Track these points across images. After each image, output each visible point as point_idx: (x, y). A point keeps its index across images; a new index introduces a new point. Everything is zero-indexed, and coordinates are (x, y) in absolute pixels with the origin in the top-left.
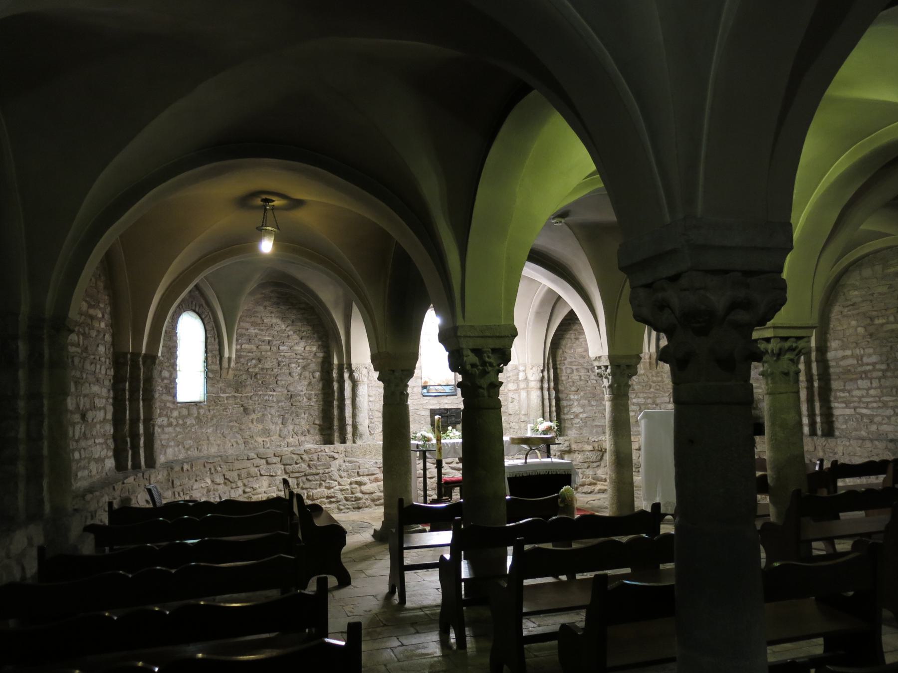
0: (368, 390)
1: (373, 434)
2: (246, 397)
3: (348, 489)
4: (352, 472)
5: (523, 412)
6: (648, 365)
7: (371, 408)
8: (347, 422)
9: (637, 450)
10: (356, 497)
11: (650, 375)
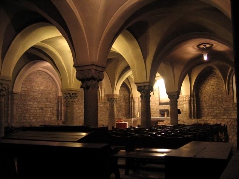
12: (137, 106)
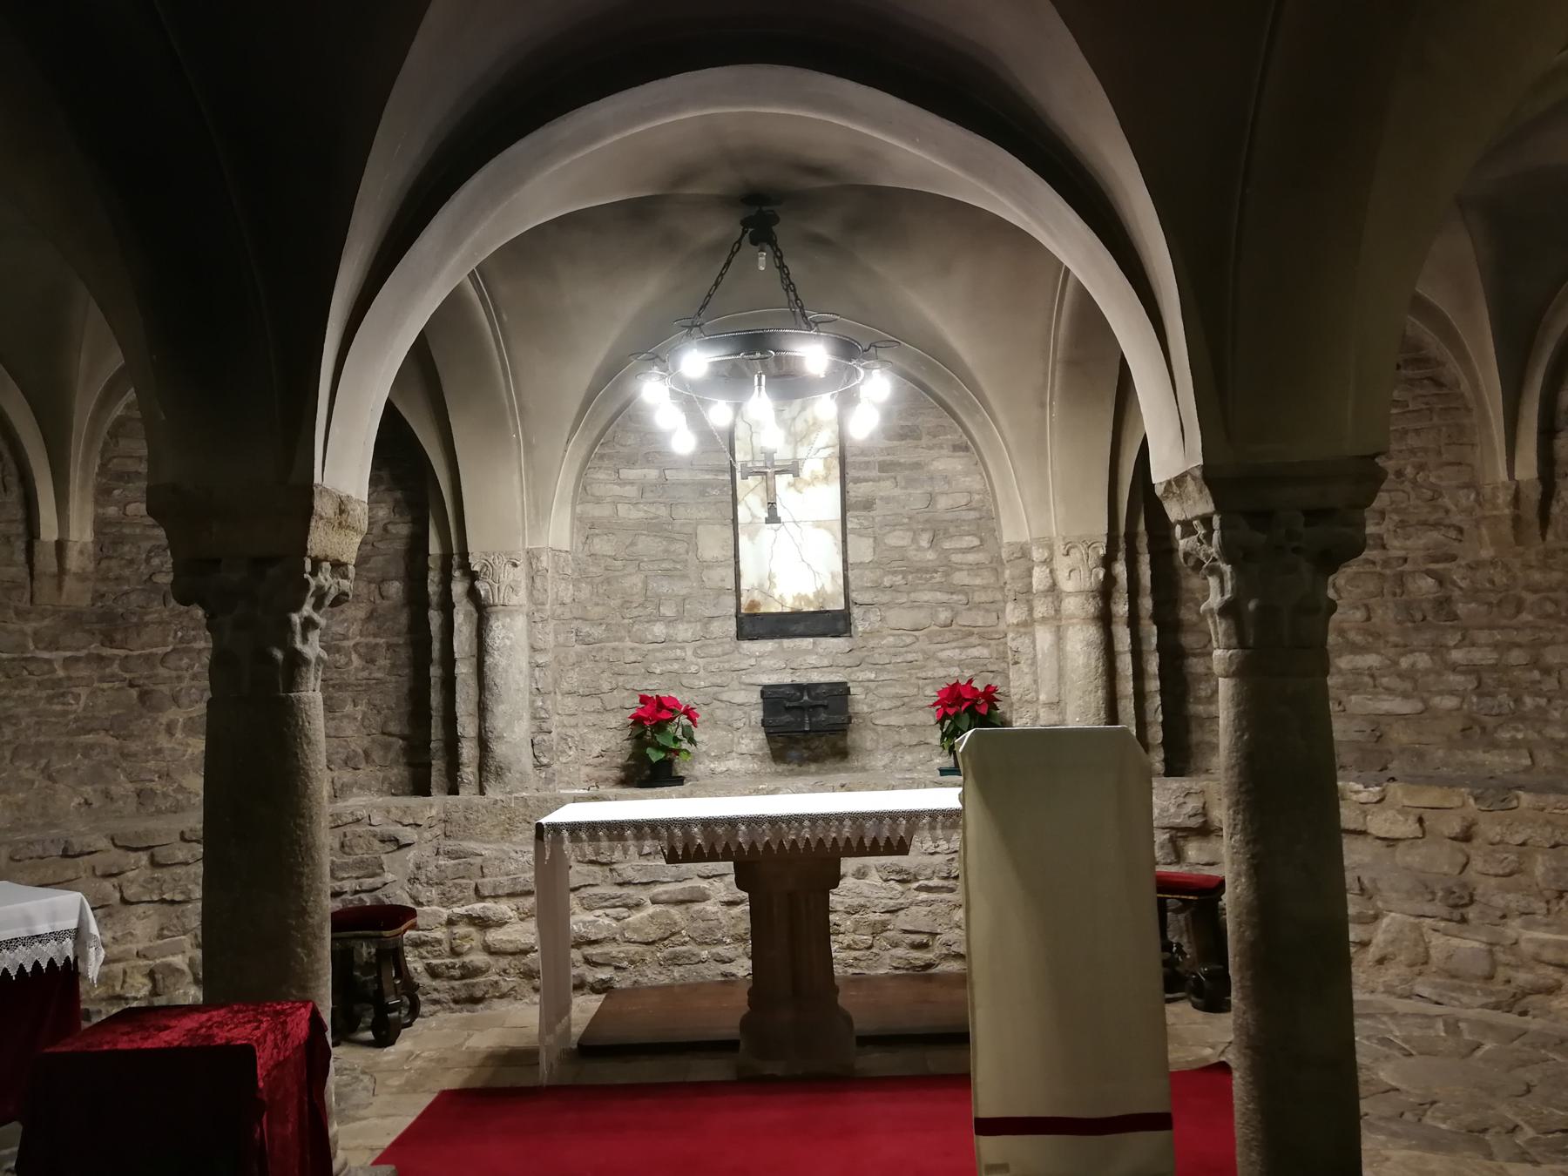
0: (530, 634)
1: (547, 766)
2: (148, 659)
3: (439, 942)
4: (455, 885)
5: (1043, 697)
6: (1506, 529)
7: (540, 687)
8: (460, 729)
9: (1454, 839)
10: (463, 966)
11: (1517, 564)
12: (522, 659)
